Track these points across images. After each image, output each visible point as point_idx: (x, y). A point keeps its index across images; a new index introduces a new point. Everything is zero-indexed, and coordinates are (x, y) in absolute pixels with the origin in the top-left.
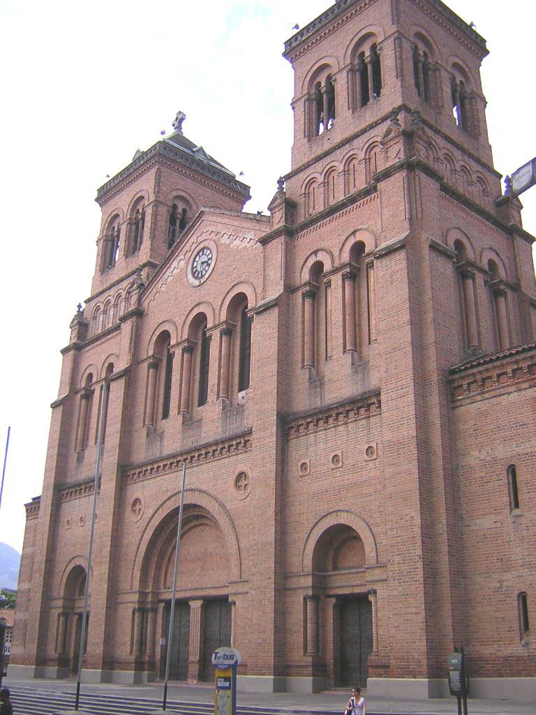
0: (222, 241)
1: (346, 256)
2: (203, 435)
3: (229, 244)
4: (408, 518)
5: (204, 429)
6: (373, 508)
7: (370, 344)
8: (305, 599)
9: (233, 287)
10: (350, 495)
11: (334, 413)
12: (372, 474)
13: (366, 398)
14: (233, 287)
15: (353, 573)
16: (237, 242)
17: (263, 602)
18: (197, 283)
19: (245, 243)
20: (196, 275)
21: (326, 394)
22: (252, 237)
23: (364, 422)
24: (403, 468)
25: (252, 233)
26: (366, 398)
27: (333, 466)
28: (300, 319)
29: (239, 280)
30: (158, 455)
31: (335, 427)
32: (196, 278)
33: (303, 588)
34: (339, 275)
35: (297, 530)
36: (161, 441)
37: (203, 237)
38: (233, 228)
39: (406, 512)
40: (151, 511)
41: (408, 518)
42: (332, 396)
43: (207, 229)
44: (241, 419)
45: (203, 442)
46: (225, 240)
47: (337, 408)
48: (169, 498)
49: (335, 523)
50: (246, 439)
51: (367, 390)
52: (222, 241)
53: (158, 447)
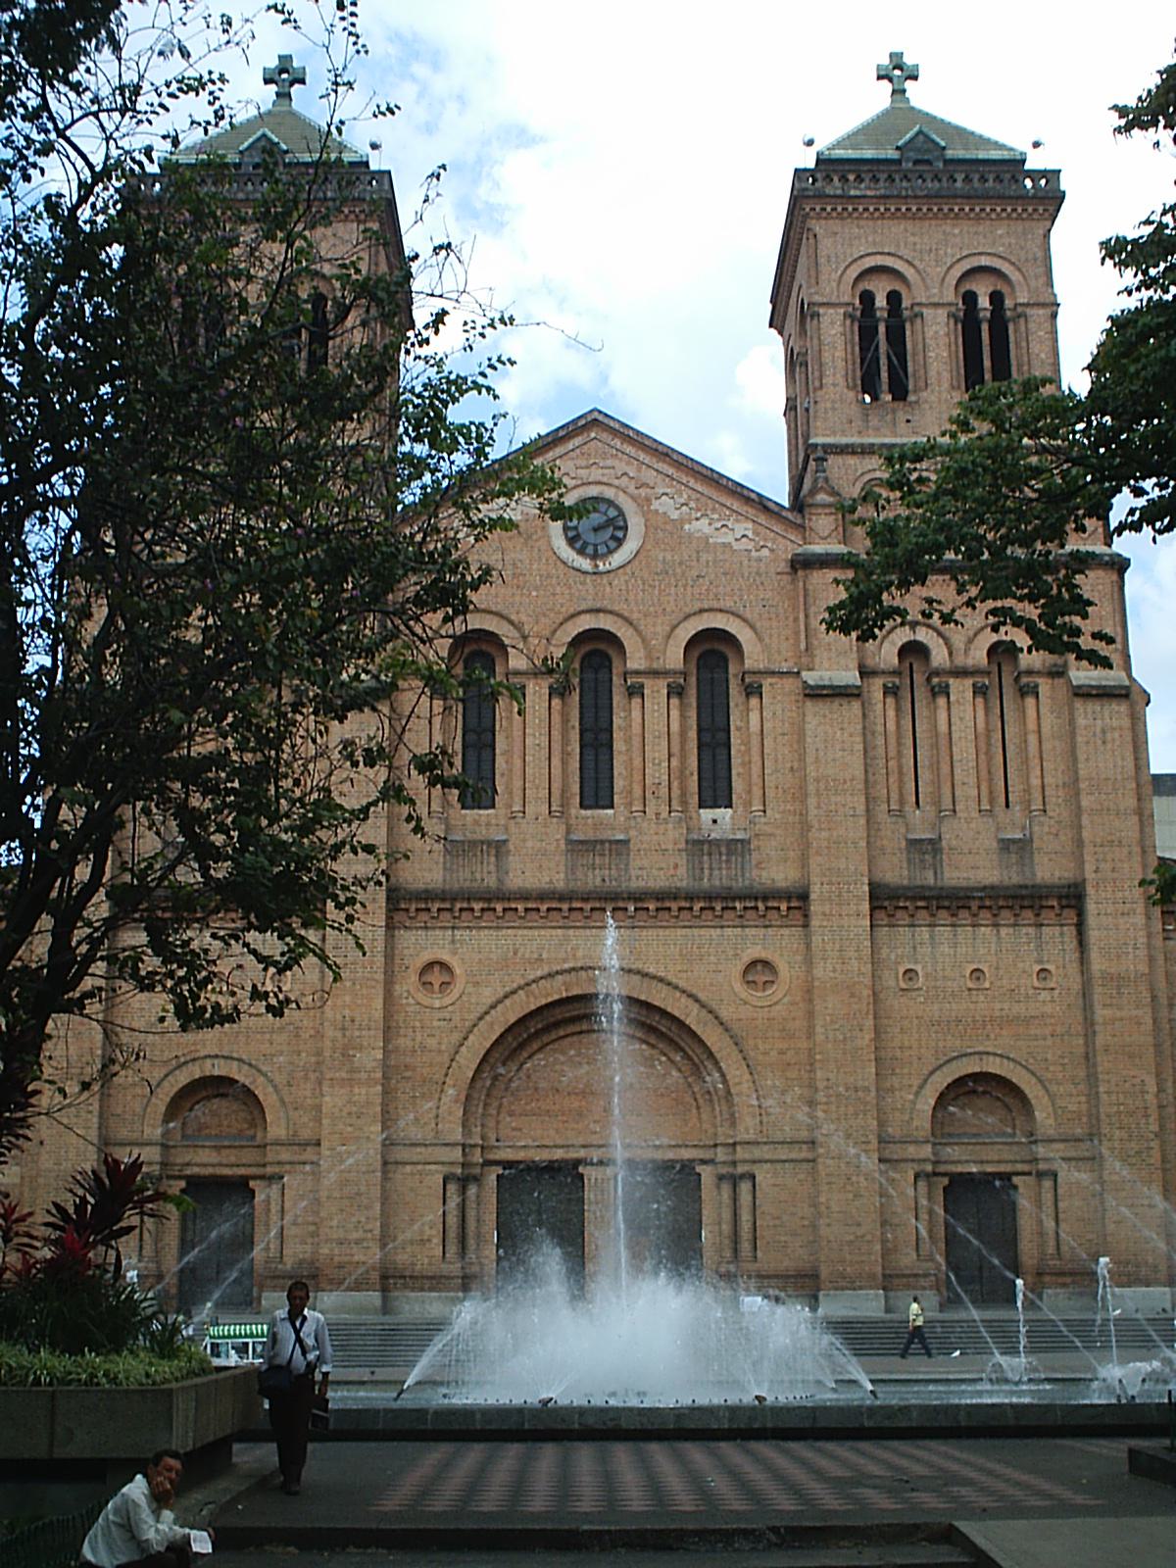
0: (655, 505)
1: (979, 656)
2: (634, 873)
3: (682, 521)
4: (1135, 1081)
5: (635, 863)
6: (1049, 1056)
7: (1007, 806)
8: (917, 1176)
9: (702, 611)
10: (1004, 1032)
11: (974, 905)
12: (1048, 1009)
13: (1040, 898)
14: (702, 611)
15: (985, 1144)
16: (702, 526)
17: (854, 1178)
18: (585, 564)
19: (730, 539)
20: (578, 545)
21: (946, 869)
22: (750, 535)
23: (1031, 930)
24: (1124, 1014)
25: (750, 525)
26: (1040, 898)
27: (970, 985)
28: (880, 728)
29: (716, 605)
30: (491, 882)
31: (974, 926)
32: (581, 552)
33: (913, 1161)
34: (969, 682)
35: (897, 1071)
36: (497, 856)
37: (596, 474)
38: (694, 496)
39: (1132, 1073)
40: (488, 995)
41: (1135, 1081)
42: (956, 874)
43: (609, 463)
44: (743, 868)
45: (635, 884)
46: (665, 505)
47: (981, 898)
48: (550, 975)
49: (977, 1069)
50: (770, 904)
51: (1029, 883)
52: (655, 505)
53: (492, 868)
